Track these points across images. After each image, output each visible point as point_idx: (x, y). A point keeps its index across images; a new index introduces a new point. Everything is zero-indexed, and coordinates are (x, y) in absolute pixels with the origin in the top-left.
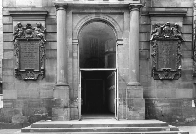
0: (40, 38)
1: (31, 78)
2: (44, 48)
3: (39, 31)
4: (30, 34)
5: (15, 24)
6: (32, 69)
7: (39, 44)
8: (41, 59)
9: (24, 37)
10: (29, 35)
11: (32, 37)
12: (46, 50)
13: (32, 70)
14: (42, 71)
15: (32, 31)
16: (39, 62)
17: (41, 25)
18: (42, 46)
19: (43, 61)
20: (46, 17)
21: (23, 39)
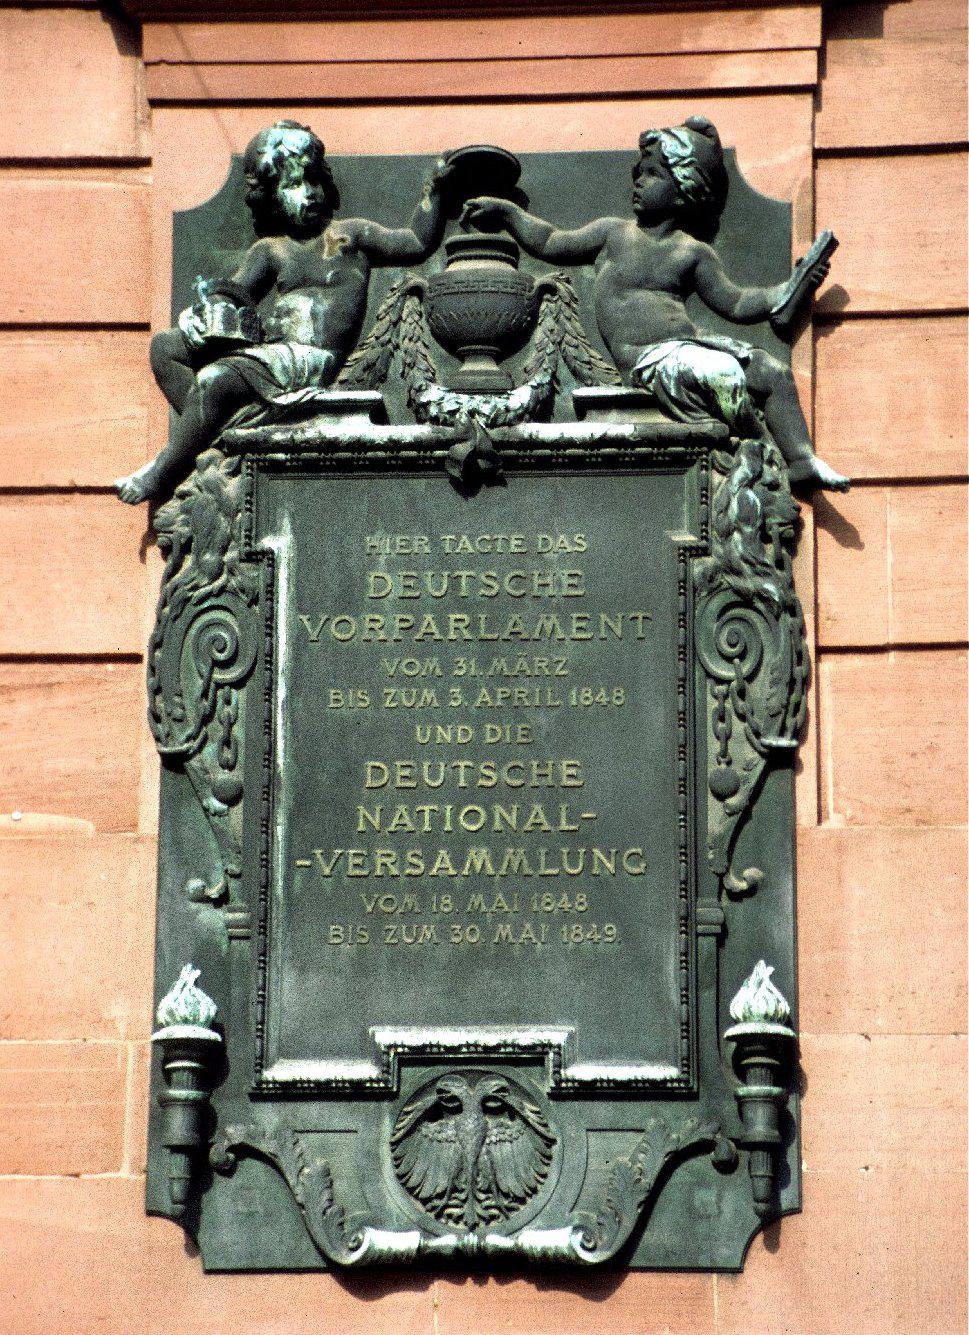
0: (708, 425)
1: (496, 1240)
2: (792, 608)
3: (687, 283)
4: (498, 359)
5: (197, 161)
6: (527, 1036)
7: (687, 538)
8: (716, 818)
9: (379, 414)
10: (480, 367)
11: (541, 410)
12: (821, 651)
13: (535, 1056)
14: (742, 1073)
15: (548, 289)
16: (690, 888)
17: (716, 166)
18: (761, 570)
19: (751, 872)
20: (830, 29)
21: (359, 445)
